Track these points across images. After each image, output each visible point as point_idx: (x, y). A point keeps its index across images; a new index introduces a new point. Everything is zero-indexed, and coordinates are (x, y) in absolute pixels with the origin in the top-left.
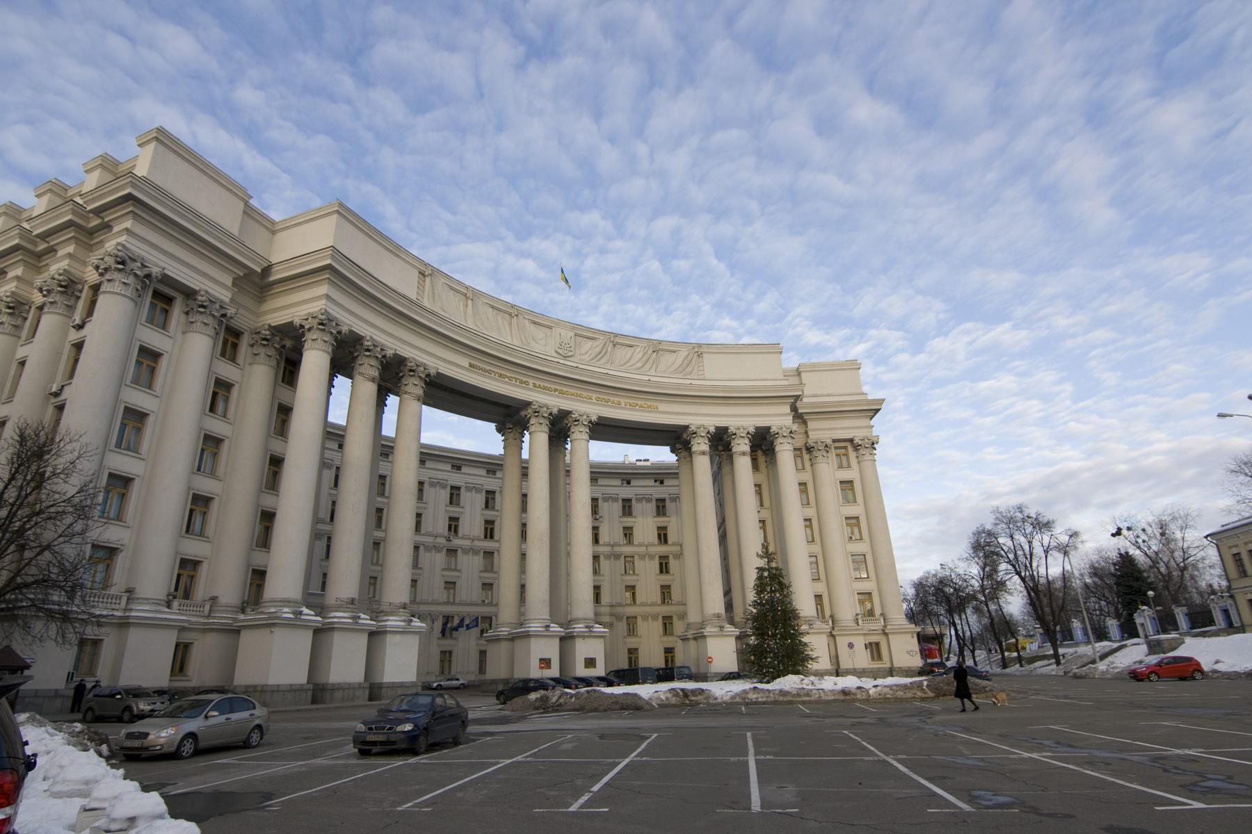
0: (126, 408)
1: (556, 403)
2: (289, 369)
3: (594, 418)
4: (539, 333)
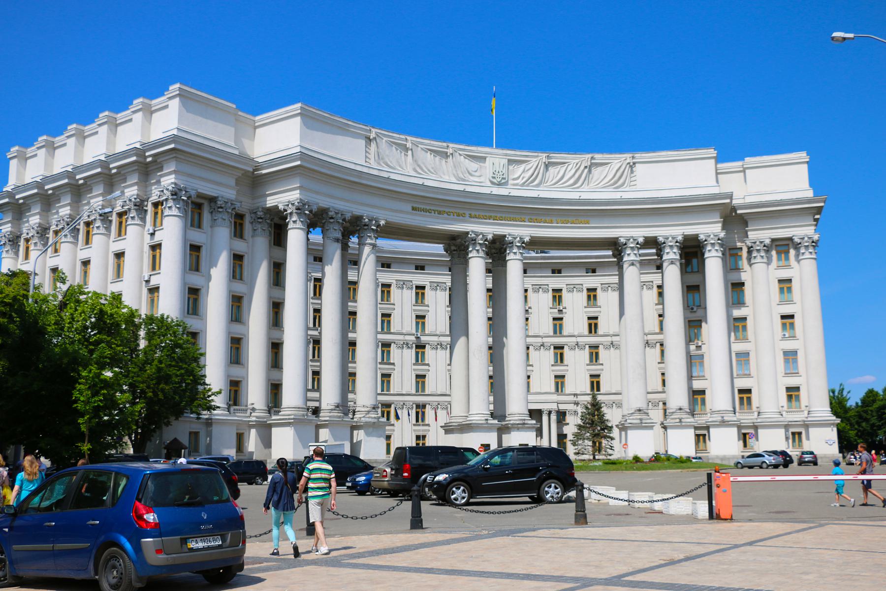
0: (189, 288)
1: (489, 230)
2: (279, 237)
3: (527, 239)
4: (473, 166)
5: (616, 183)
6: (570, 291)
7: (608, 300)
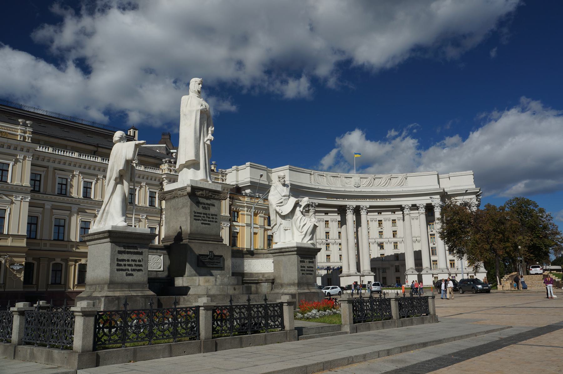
3: (368, 207)
4: (348, 180)
5: (400, 184)
6: (385, 220)
7: (399, 223)
